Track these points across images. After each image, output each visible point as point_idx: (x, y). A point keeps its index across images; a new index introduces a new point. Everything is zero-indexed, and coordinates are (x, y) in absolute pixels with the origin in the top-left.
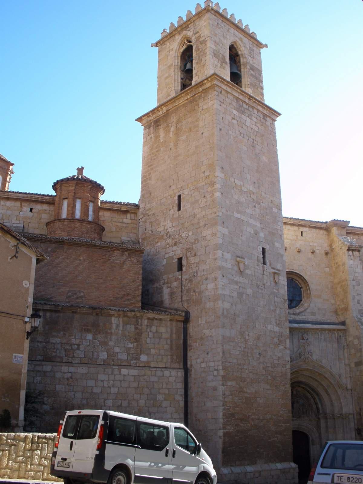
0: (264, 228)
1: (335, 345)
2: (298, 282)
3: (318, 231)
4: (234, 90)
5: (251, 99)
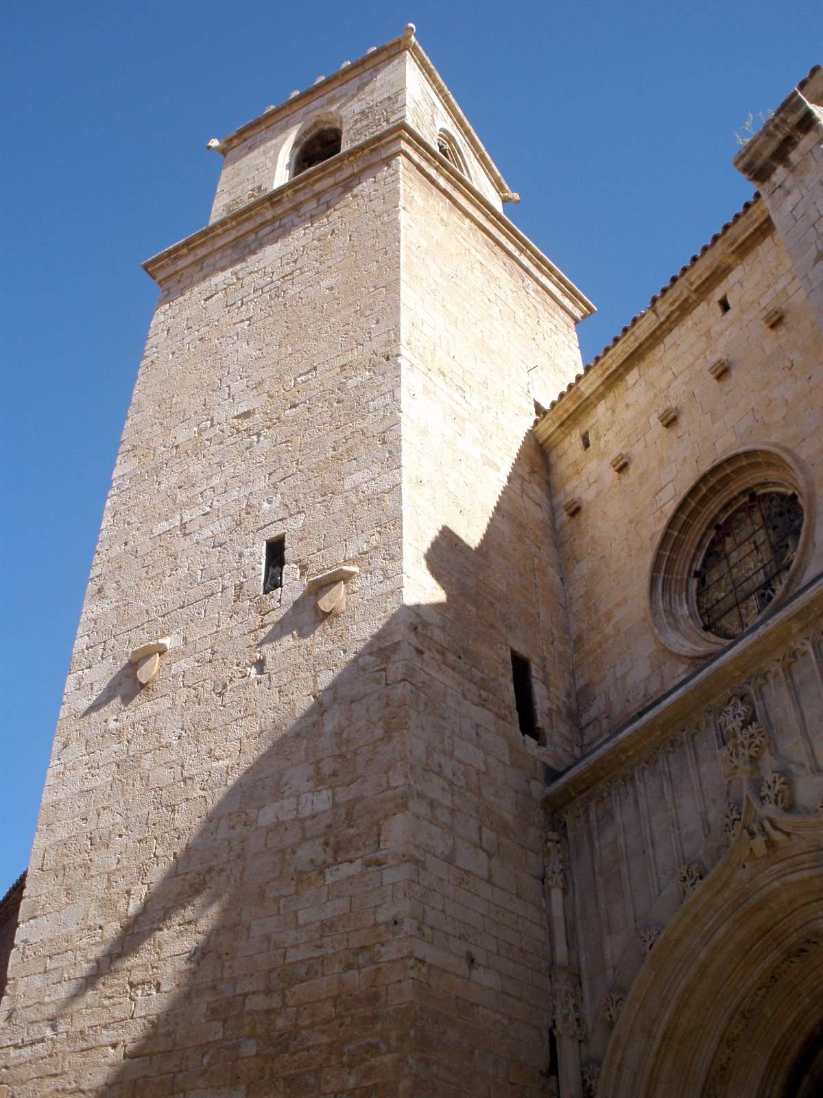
4: (218, 235)
5: (279, 197)
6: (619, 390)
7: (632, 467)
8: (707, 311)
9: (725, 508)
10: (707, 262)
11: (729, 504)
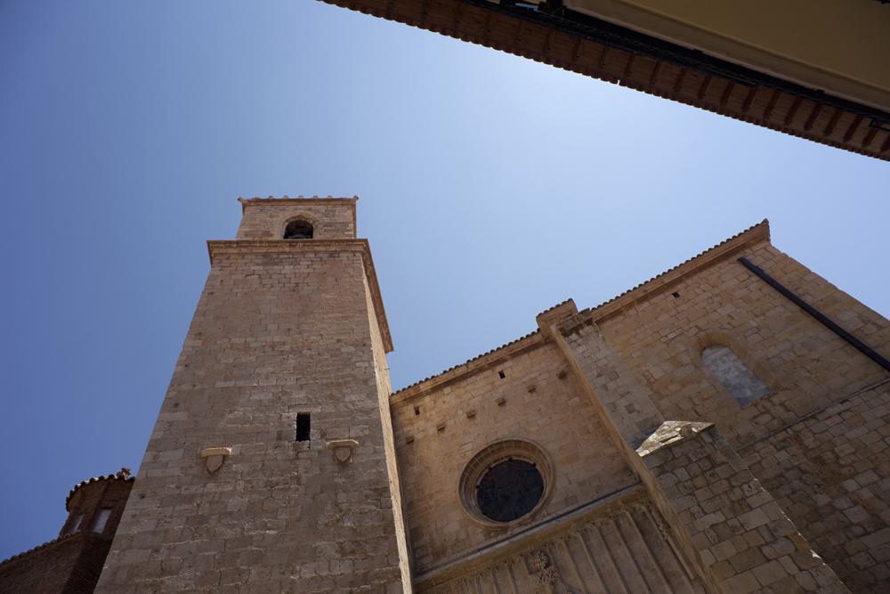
1: (639, 544)
2: (524, 457)
3: (532, 354)
6: (439, 393)
7: (446, 430)
8: (493, 375)
9: (495, 461)
11: (498, 460)
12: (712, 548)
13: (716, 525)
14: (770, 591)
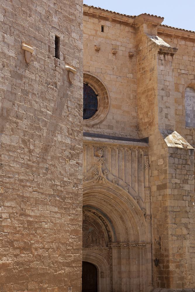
0: (60, 10)
1: (136, 165)
2: (94, 88)
3: (122, 27)
10: (108, 14)
12: (172, 190)
13: (177, 183)
14: (179, 208)
